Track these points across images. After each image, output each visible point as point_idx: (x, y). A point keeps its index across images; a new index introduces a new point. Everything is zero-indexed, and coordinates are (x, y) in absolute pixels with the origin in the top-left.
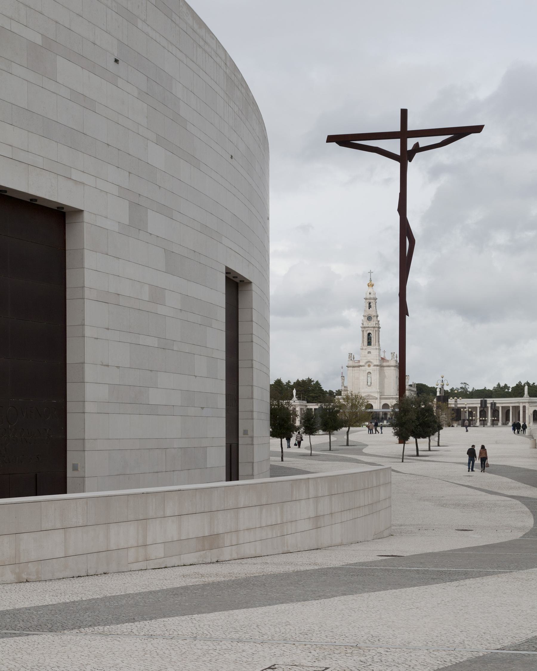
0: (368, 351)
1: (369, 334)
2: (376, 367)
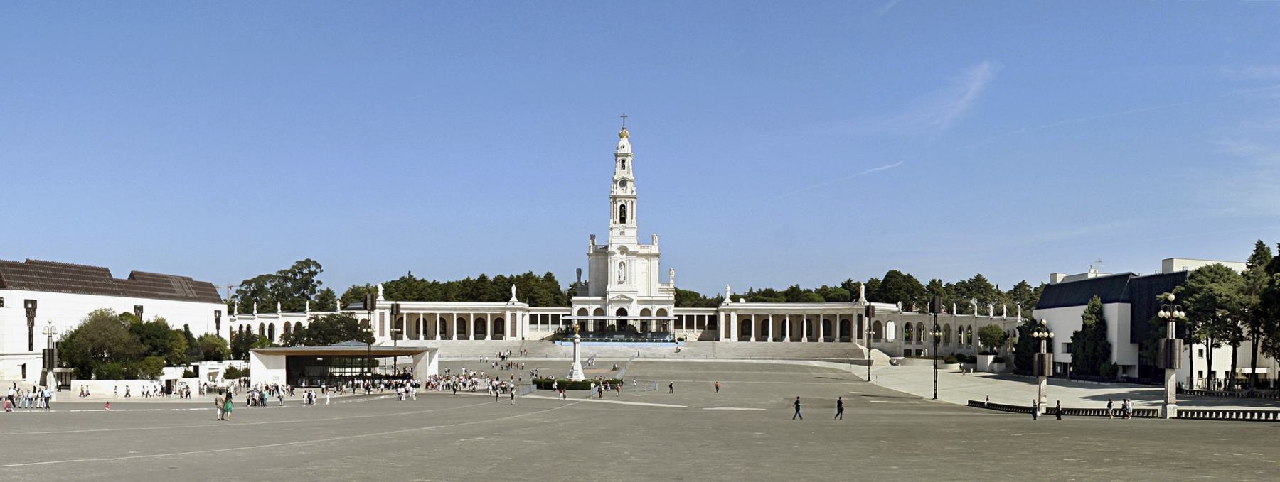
1: (623, 207)
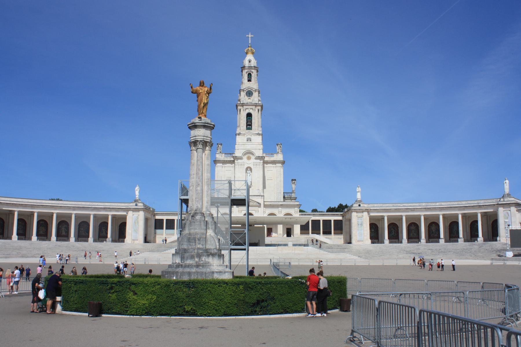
0: (247, 137)
1: (249, 115)
2: (258, 161)
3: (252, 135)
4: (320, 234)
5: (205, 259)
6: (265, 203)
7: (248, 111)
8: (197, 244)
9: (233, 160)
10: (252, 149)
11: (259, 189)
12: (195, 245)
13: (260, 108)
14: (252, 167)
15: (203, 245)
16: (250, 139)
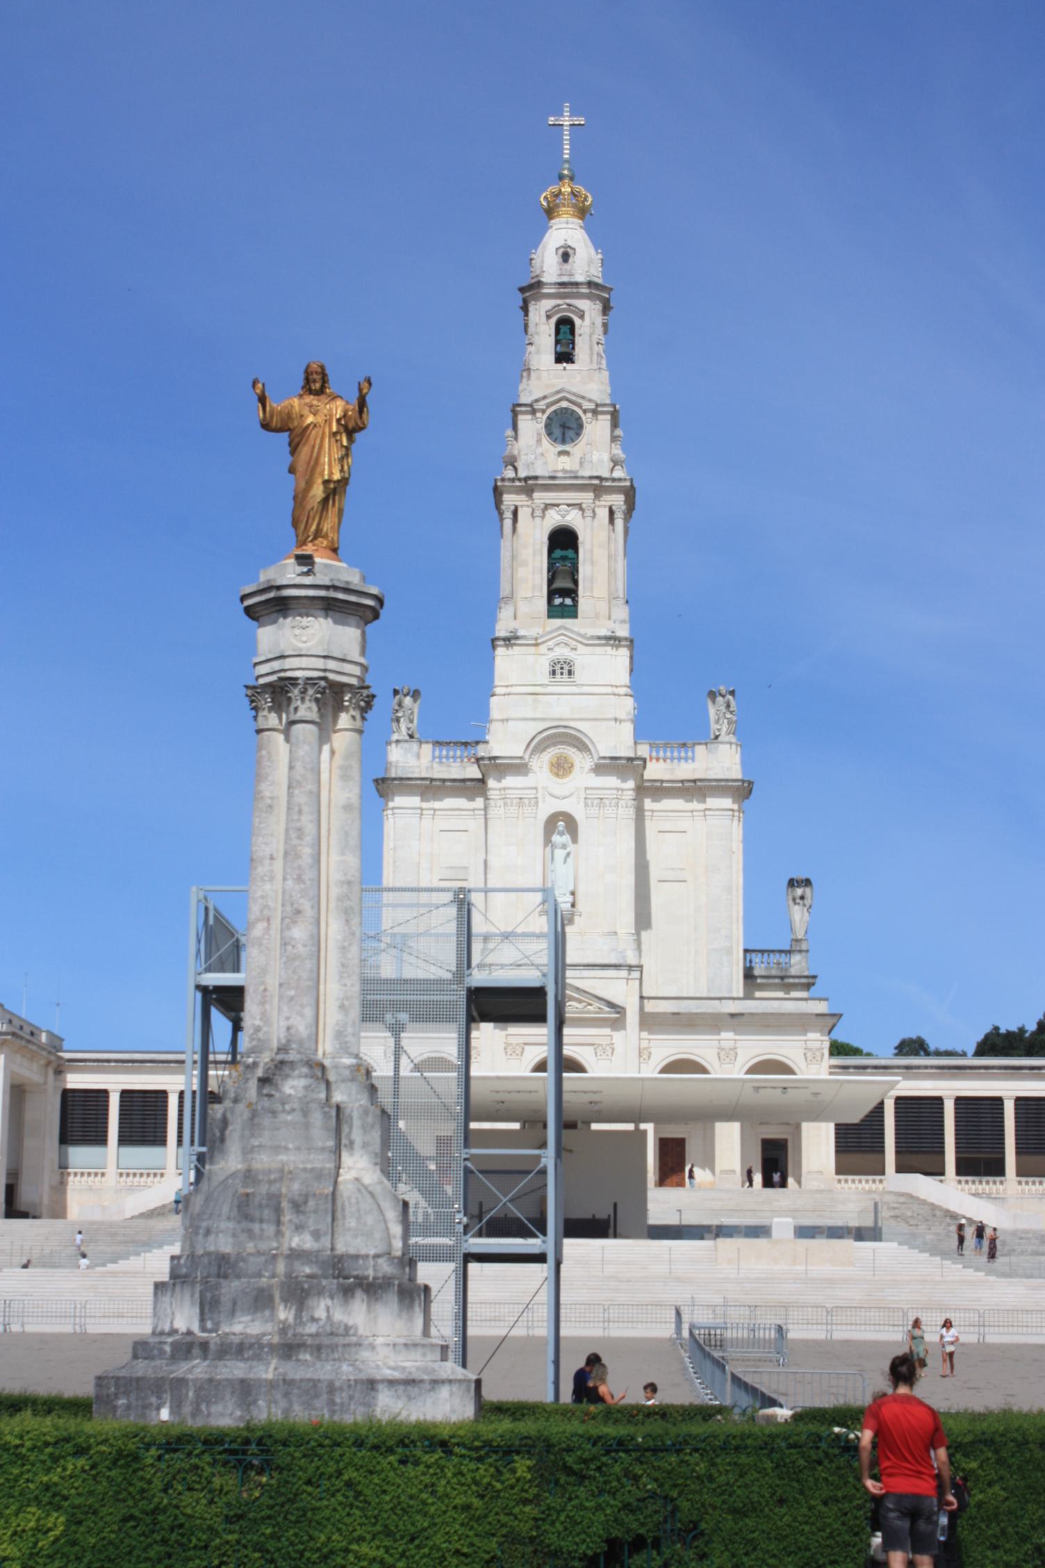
2: (612, 781)
3: (579, 646)
4: (942, 1174)
5: (328, 1310)
6: (650, 1007)
7: (558, 518)
8: (287, 1231)
9: (479, 776)
10: (576, 716)
11: (615, 933)
12: (279, 1233)
13: (618, 500)
14: (578, 813)
15: (316, 1235)
16: (566, 668)
